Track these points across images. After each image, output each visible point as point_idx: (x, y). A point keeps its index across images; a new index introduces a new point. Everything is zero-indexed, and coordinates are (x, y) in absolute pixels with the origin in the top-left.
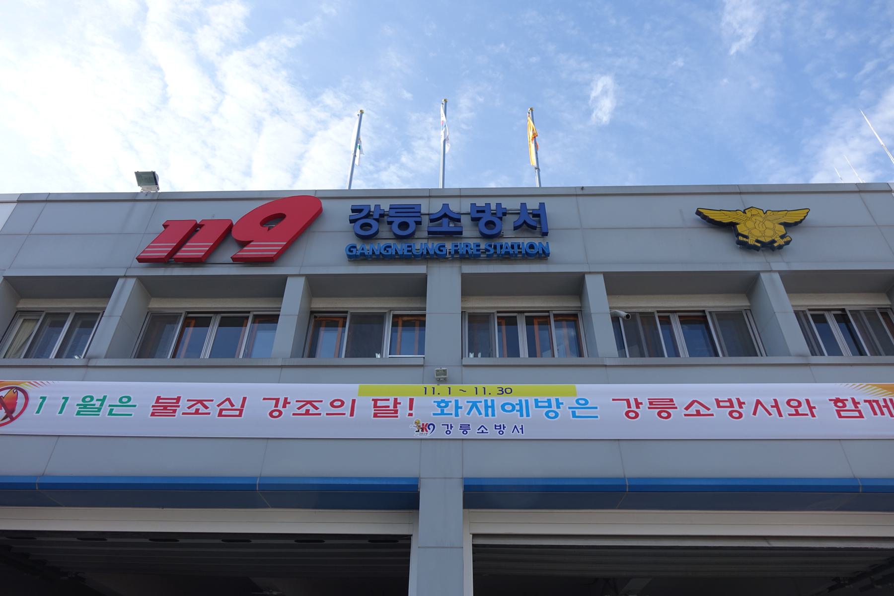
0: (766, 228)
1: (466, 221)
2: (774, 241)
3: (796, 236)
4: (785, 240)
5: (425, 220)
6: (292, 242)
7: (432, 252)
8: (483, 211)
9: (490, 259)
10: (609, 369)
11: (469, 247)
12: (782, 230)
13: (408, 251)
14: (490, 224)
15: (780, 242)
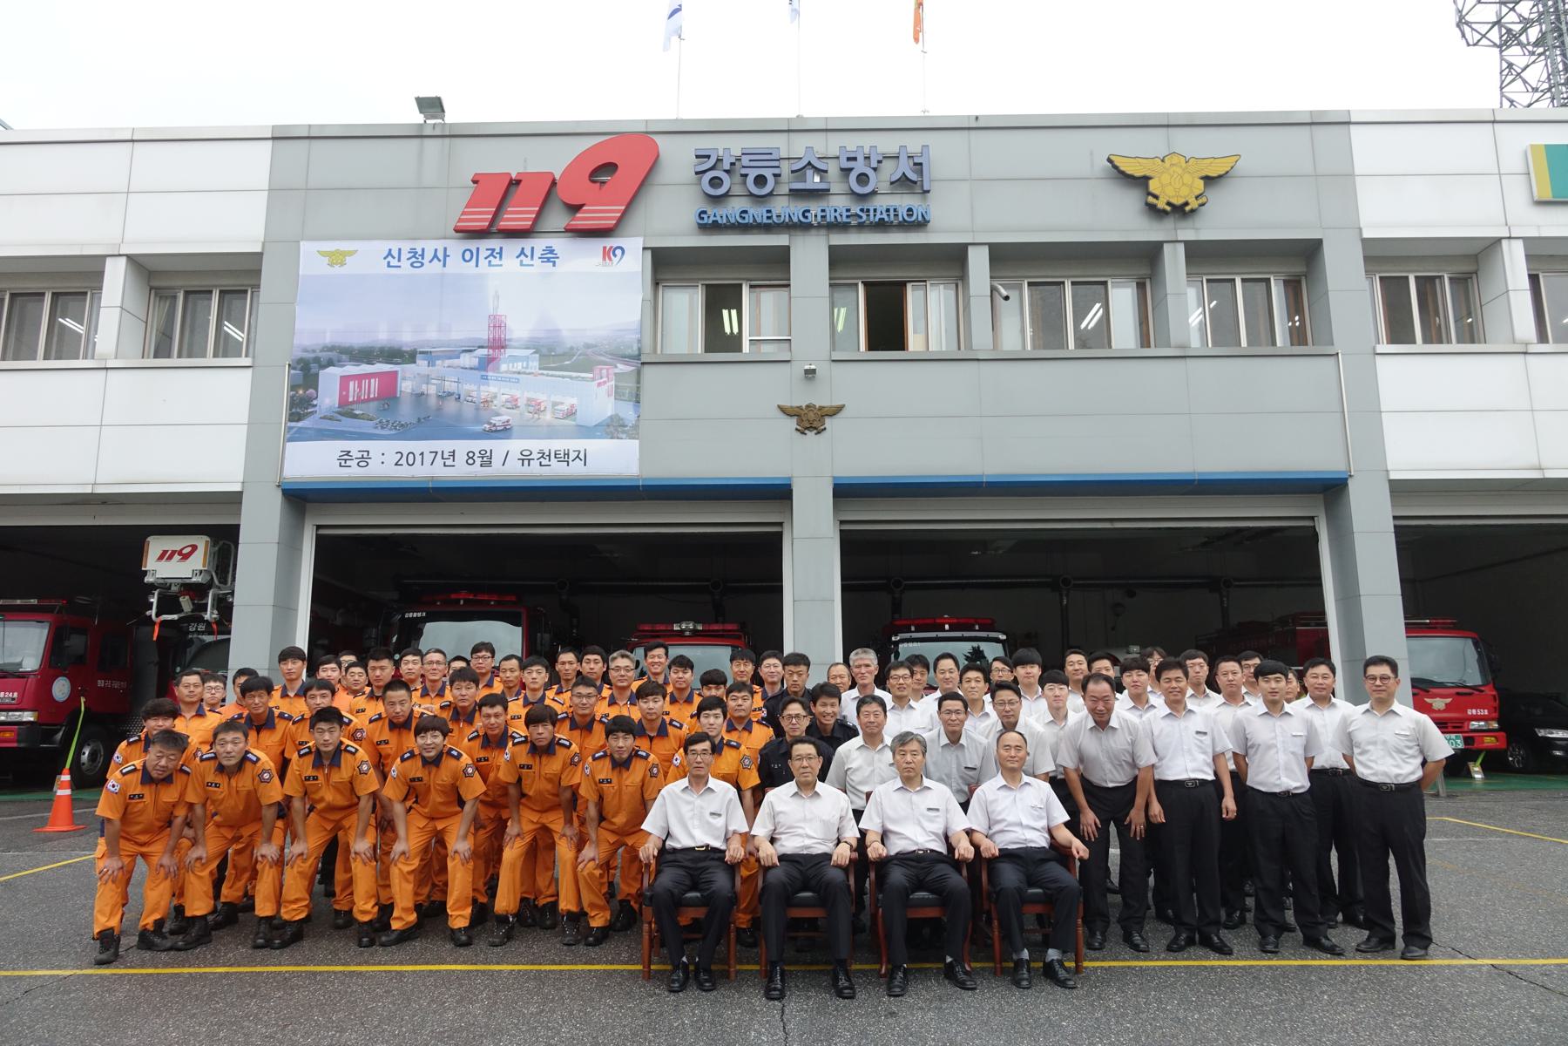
0: (1183, 184)
1: (833, 169)
2: (1187, 204)
3: (1215, 197)
4: (1200, 201)
5: (785, 169)
6: (629, 205)
7: (795, 220)
8: (855, 159)
9: (861, 227)
10: (982, 364)
11: (839, 211)
12: (1200, 185)
13: (768, 218)
14: (863, 179)
15: (1194, 204)
